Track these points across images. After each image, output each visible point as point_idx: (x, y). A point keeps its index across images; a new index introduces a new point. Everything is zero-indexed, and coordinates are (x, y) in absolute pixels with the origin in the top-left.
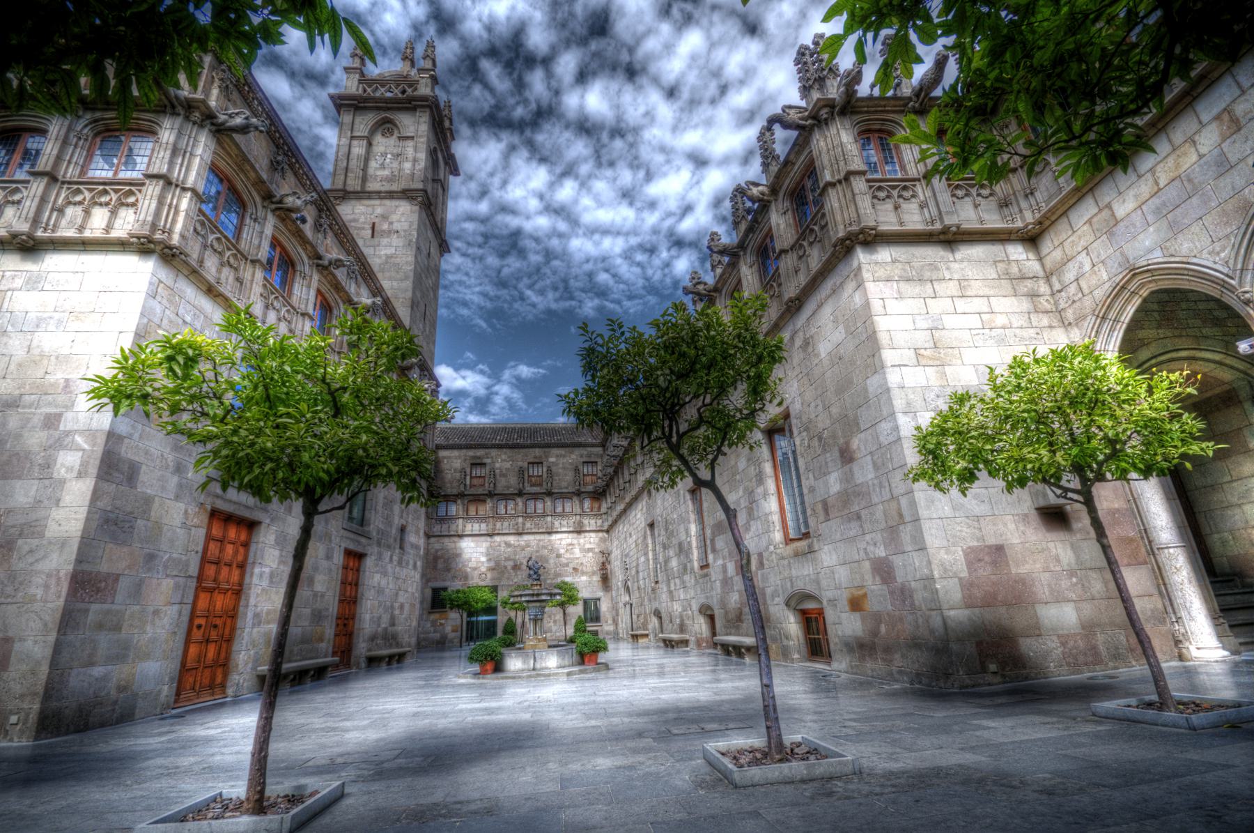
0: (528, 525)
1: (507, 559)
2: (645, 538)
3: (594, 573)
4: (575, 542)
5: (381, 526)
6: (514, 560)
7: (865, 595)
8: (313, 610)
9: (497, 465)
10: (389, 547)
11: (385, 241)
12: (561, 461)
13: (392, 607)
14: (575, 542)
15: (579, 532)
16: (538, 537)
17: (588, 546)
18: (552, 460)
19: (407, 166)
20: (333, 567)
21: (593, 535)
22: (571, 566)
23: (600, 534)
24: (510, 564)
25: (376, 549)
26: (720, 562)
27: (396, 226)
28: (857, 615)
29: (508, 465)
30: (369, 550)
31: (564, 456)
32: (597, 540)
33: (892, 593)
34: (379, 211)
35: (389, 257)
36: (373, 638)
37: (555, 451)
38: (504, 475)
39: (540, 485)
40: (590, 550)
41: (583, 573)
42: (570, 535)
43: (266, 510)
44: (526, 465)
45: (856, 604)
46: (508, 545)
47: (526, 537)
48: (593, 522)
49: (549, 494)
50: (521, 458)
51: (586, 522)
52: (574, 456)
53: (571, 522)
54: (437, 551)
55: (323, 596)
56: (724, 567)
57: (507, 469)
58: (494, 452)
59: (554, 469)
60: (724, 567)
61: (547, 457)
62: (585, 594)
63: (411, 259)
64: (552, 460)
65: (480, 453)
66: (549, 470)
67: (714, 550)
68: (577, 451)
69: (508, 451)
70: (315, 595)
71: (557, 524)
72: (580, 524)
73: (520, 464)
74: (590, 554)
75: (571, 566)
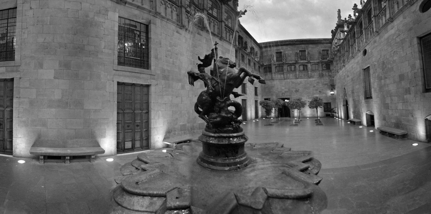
17: (325, 83)
18: (310, 49)
24: (295, 90)
29: (291, 52)
40: (326, 84)
44: (298, 51)
46: (293, 83)
50: (297, 49)
52: (318, 48)
58: (284, 47)
69: (291, 46)
73: (296, 51)
74: (326, 86)
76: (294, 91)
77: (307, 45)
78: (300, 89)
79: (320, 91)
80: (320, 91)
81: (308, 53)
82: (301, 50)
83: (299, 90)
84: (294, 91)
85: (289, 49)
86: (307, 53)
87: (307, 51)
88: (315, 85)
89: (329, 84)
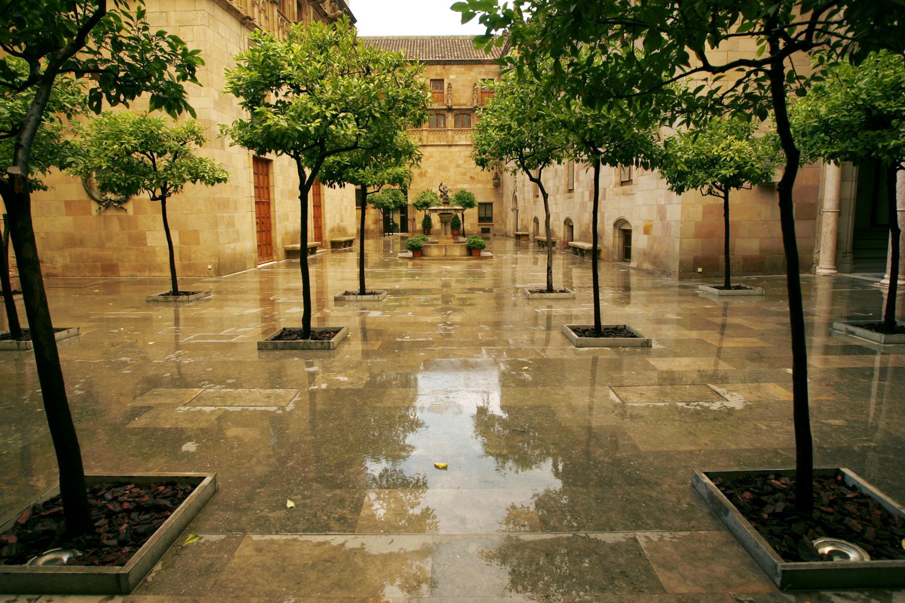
3: (488, 182)
7: (651, 226)
13: (341, 209)
16: (440, 149)
22: (469, 175)
26: (580, 190)
28: (646, 236)
31: (464, 74)
33: (663, 226)
41: (479, 182)
45: (647, 231)
56: (583, 193)
60: (583, 193)
61: (448, 74)
62: (479, 198)
64: (452, 77)
67: (578, 180)
68: (477, 69)
71: (456, 137)
78: (430, 170)
81: (450, 86)
83: (426, 172)
86: (446, 86)
87: (446, 81)
88: (461, 162)
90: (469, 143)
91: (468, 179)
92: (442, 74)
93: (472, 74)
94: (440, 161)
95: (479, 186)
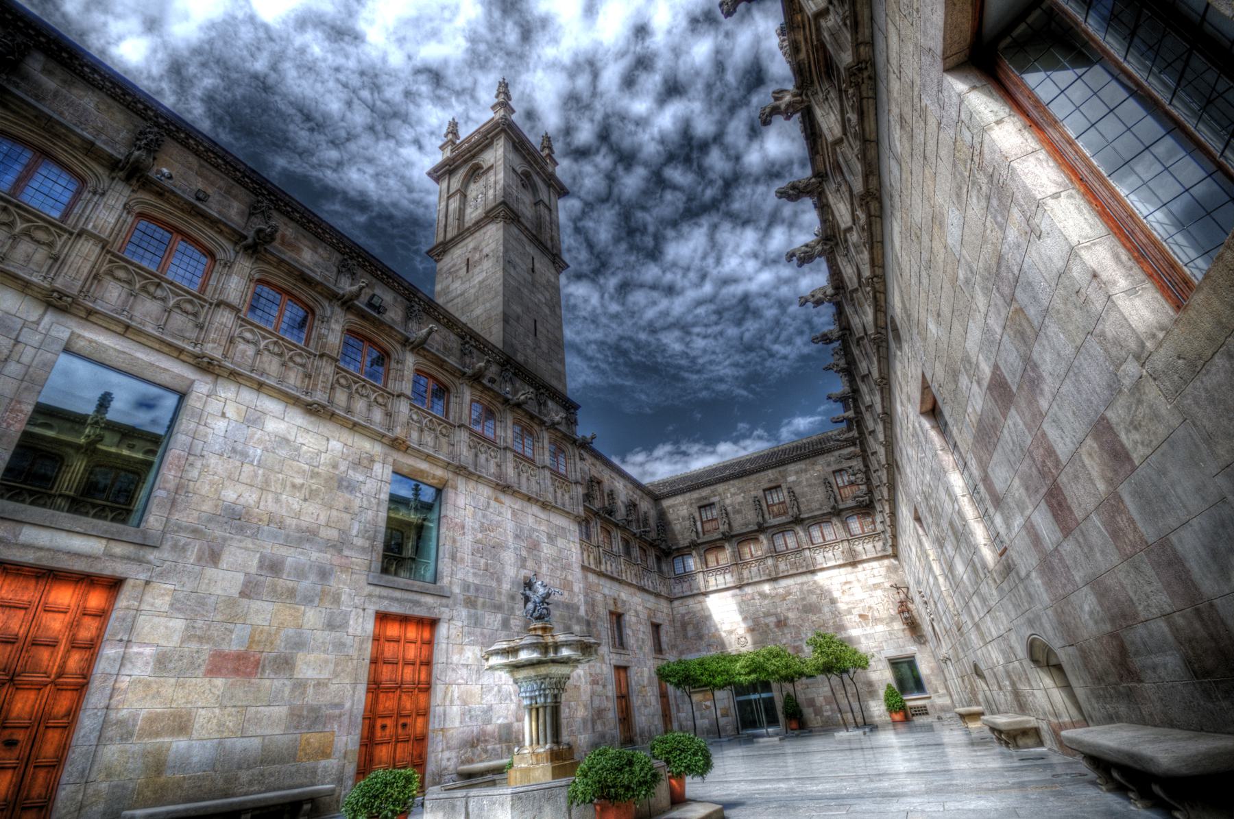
0: (782, 566)
1: (767, 615)
2: (920, 541)
3: (892, 619)
4: (851, 578)
5: (470, 579)
6: (776, 615)
8: (292, 708)
9: (728, 502)
10: (498, 608)
11: (477, 270)
12: (804, 477)
14: (851, 578)
15: (854, 564)
16: (799, 580)
18: (792, 478)
19: (491, 192)
20: (349, 640)
21: (875, 564)
22: (856, 612)
23: (886, 562)
24: (773, 619)
25: (464, 613)
27: (486, 250)
29: (740, 498)
30: (445, 613)
31: (806, 471)
32: (883, 571)
34: (471, 246)
35: (481, 283)
36: (474, 742)
37: (792, 468)
38: (739, 512)
39: (786, 513)
40: (876, 586)
41: (877, 621)
42: (842, 570)
43: (140, 561)
44: (760, 493)
46: (763, 596)
47: (784, 583)
48: (869, 546)
49: (798, 521)
50: (754, 486)
51: (859, 548)
53: (838, 552)
54: (683, 616)
55: (319, 684)
57: (741, 504)
58: (720, 488)
59: (797, 490)
61: (784, 477)
63: (500, 274)
64: (792, 478)
65: (706, 492)
66: (791, 491)
68: (821, 460)
69: (736, 482)
70: (300, 685)
71: (819, 558)
72: (852, 552)
73: (753, 493)
74: (879, 593)
75: (856, 612)
76: (772, 625)
77: (781, 469)
78: (791, 615)
79: (861, 616)
80: (861, 616)
82: (767, 486)
83: (786, 618)
84: (772, 625)
85: (732, 490)
87: (784, 486)
89: (887, 585)
90: (841, 562)
91: (858, 619)
92: (777, 479)
93: (818, 468)
94: (803, 599)
95: (881, 628)
